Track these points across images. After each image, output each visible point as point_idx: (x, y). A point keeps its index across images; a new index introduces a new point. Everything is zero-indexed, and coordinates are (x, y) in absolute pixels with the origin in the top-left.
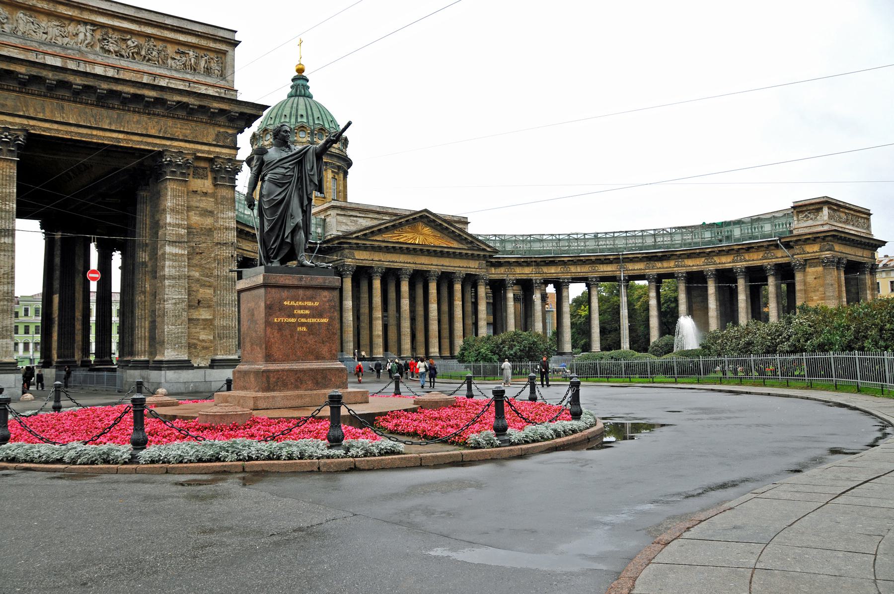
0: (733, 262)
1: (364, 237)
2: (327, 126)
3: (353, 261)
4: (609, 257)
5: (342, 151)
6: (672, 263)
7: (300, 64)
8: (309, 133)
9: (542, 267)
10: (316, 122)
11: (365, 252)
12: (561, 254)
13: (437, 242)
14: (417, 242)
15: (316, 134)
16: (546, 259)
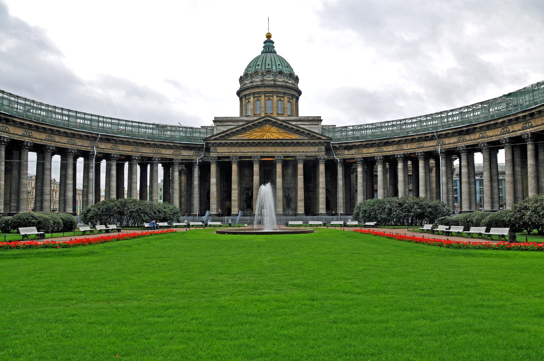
0: (523, 129)
1: (223, 138)
2: (274, 68)
3: (216, 154)
4: (428, 135)
5: (287, 82)
6: (477, 135)
7: (269, 33)
8: (260, 75)
9: (383, 147)
10: (267, 67)
11: (224, 148)
12: (394, 136)
13: (280, 138)
14: (264, 138)
15: (265, 75)
16: (382, 141)
